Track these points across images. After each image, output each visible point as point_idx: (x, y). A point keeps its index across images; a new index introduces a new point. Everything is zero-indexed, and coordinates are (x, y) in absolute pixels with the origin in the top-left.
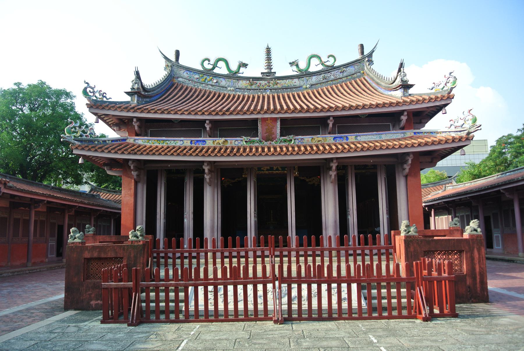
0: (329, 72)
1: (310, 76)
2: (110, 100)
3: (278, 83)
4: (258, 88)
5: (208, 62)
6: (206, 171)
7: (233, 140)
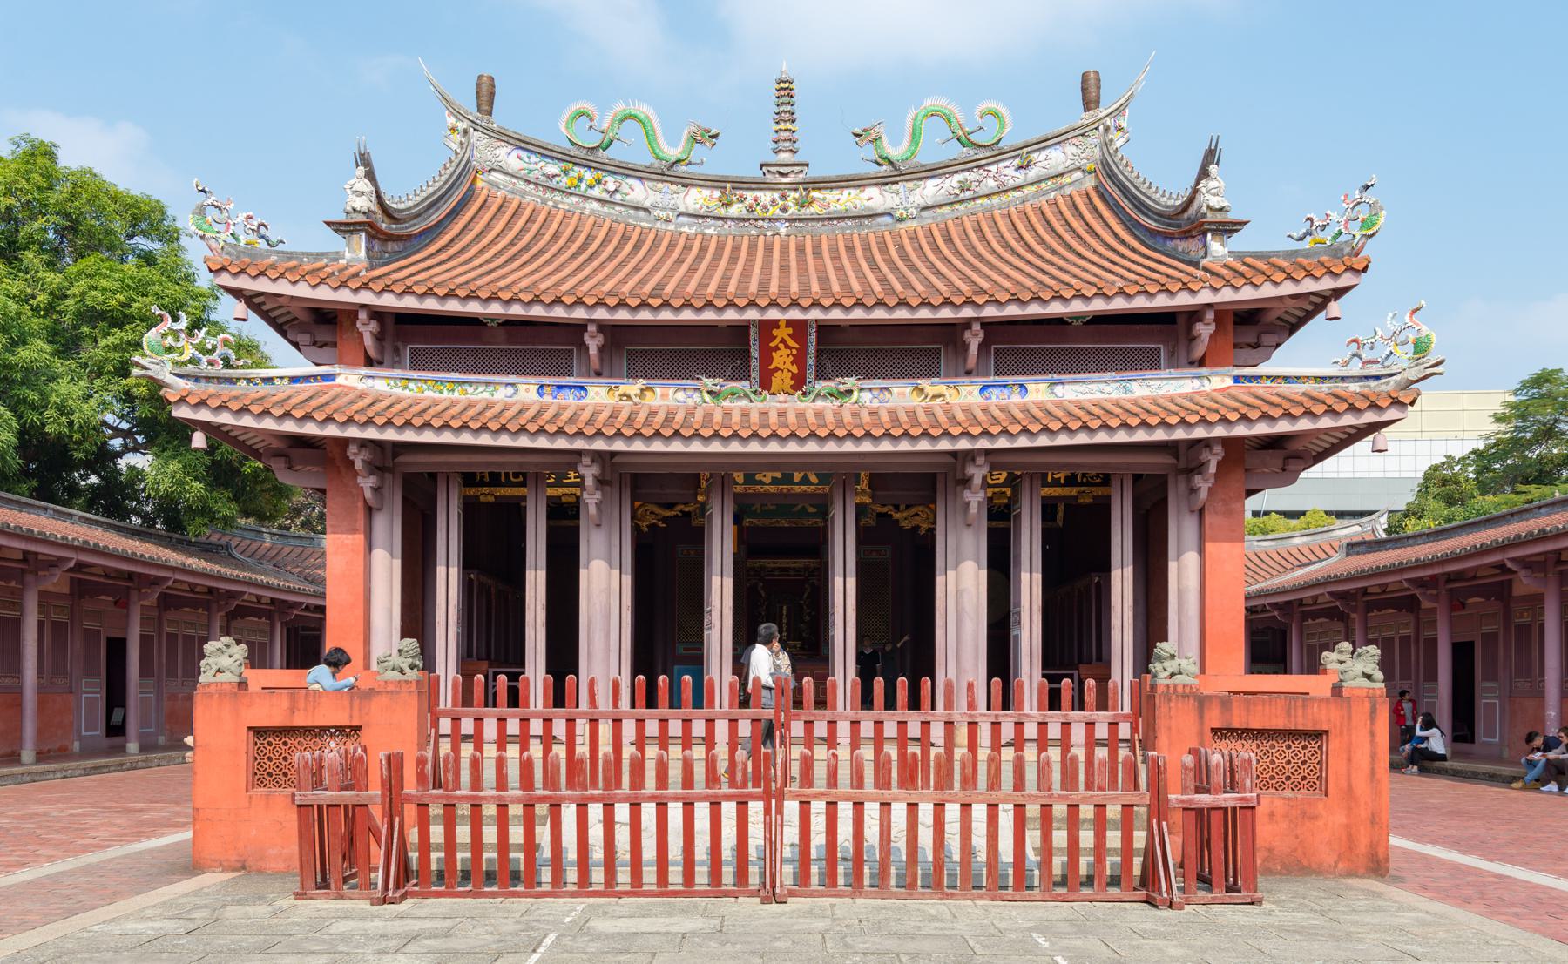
0: (979, 167)
1: (920, 179)
2: (280, 247)
3: (813, 200)
4: (751, 216)
6: (589, 482)
7: (669, 386)
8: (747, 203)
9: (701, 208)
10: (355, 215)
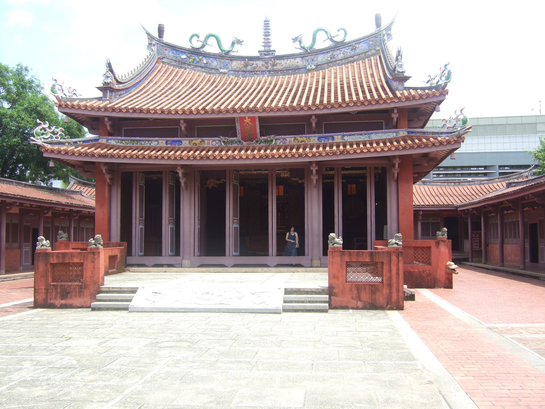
0: (338, 50)
1: (316, 55)
3: (277, 64)
5: (197, 39)
7: (210, 140)
9: (237, 68)
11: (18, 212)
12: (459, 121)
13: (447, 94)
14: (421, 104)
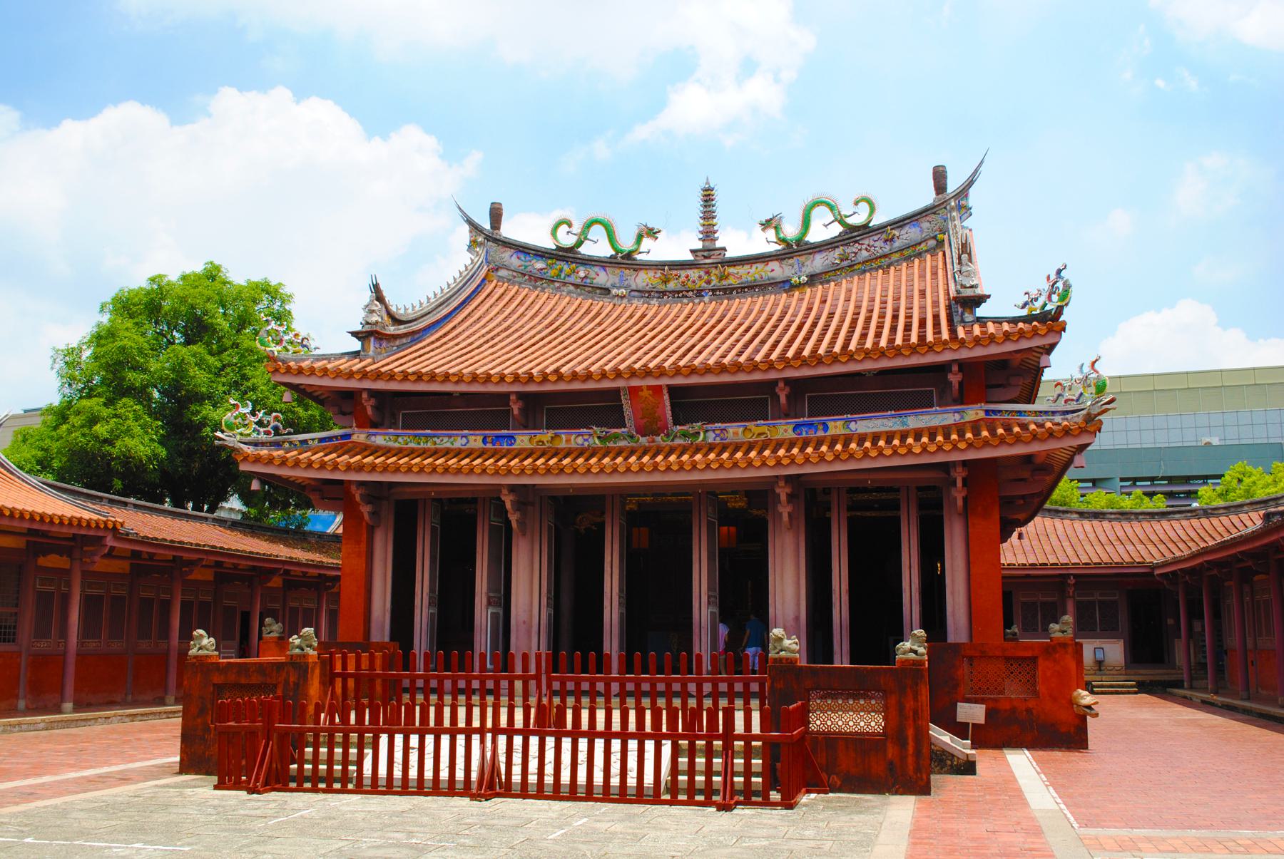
1: (810, 254)
3: (729, 274)
4: (683, 289)
5: (568, 229)
8: (682, 279)
10: (367, 326)
11: (211, 578)
12: (1089, 386)
13: (1064, 330)
14: (1010, 353)
